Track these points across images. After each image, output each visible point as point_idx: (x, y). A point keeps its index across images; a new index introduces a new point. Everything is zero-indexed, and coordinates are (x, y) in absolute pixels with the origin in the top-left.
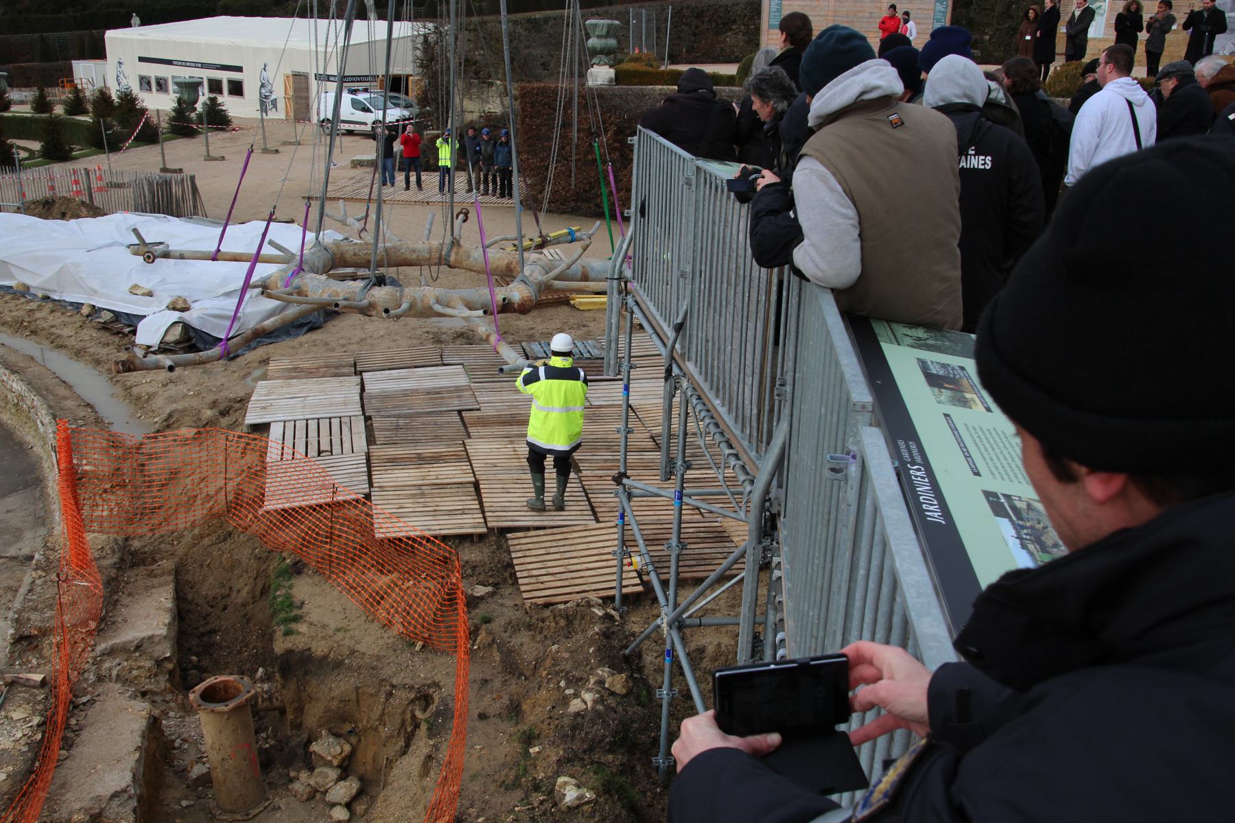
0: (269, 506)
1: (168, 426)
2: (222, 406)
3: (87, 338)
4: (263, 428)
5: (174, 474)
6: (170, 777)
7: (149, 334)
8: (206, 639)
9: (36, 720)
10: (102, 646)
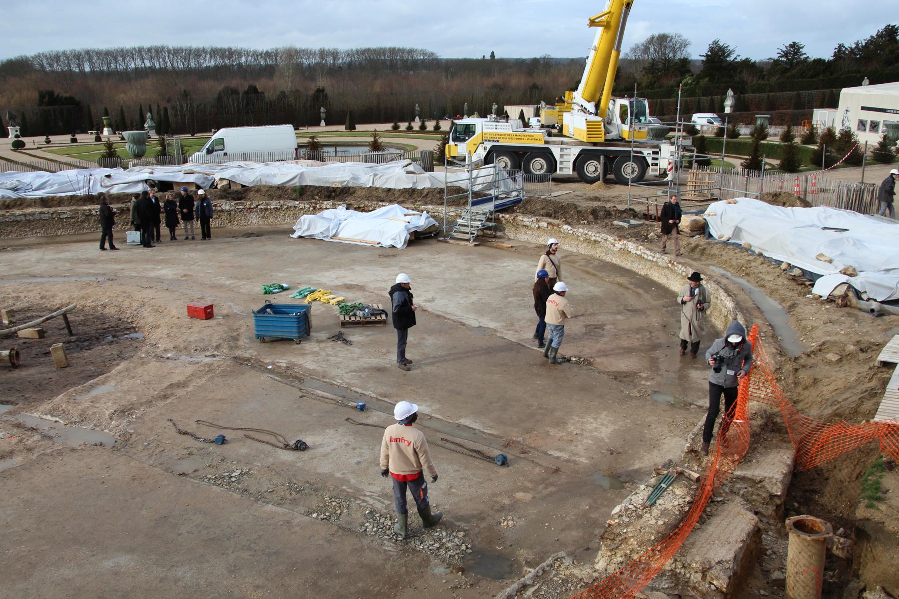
0: (877, 418)
1: (820, 350)
2: (862, 346)
3: (780, 283)
4: (889, 366)
5: (815, 381)
6: (758, 571)
7: (822, 288)
8: (808, 494)
9: (688, 499)
10: (738, 473)
